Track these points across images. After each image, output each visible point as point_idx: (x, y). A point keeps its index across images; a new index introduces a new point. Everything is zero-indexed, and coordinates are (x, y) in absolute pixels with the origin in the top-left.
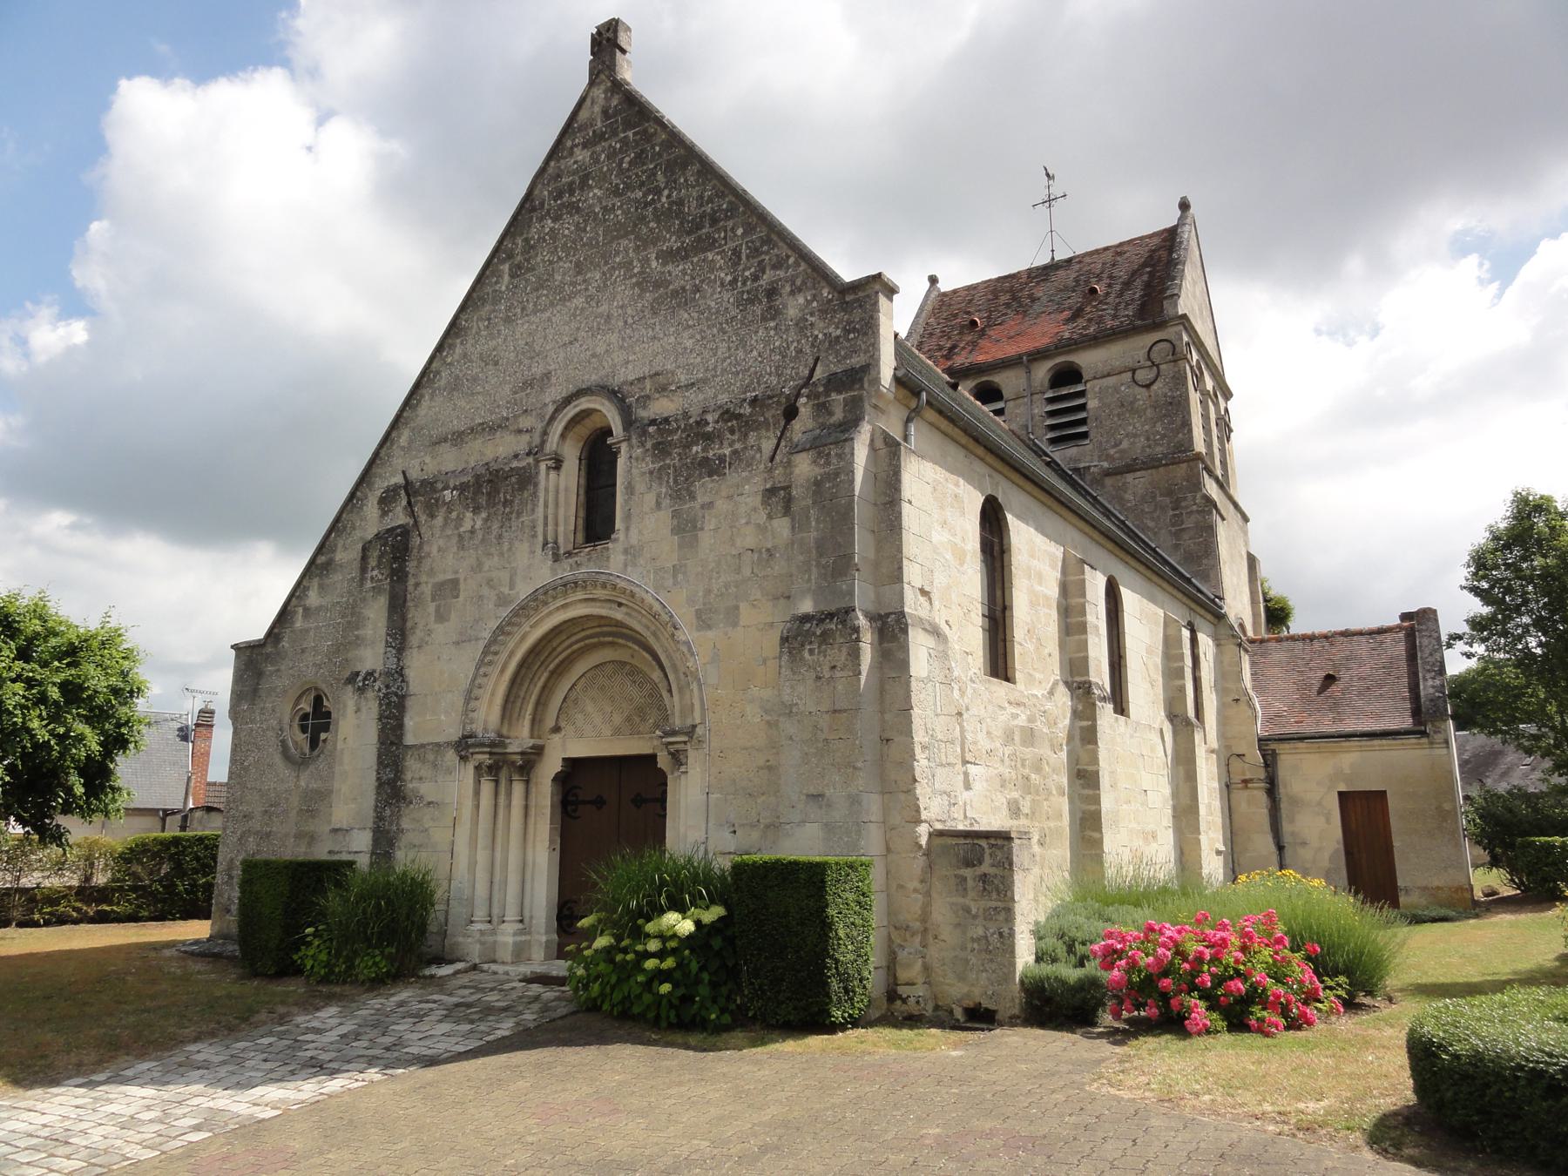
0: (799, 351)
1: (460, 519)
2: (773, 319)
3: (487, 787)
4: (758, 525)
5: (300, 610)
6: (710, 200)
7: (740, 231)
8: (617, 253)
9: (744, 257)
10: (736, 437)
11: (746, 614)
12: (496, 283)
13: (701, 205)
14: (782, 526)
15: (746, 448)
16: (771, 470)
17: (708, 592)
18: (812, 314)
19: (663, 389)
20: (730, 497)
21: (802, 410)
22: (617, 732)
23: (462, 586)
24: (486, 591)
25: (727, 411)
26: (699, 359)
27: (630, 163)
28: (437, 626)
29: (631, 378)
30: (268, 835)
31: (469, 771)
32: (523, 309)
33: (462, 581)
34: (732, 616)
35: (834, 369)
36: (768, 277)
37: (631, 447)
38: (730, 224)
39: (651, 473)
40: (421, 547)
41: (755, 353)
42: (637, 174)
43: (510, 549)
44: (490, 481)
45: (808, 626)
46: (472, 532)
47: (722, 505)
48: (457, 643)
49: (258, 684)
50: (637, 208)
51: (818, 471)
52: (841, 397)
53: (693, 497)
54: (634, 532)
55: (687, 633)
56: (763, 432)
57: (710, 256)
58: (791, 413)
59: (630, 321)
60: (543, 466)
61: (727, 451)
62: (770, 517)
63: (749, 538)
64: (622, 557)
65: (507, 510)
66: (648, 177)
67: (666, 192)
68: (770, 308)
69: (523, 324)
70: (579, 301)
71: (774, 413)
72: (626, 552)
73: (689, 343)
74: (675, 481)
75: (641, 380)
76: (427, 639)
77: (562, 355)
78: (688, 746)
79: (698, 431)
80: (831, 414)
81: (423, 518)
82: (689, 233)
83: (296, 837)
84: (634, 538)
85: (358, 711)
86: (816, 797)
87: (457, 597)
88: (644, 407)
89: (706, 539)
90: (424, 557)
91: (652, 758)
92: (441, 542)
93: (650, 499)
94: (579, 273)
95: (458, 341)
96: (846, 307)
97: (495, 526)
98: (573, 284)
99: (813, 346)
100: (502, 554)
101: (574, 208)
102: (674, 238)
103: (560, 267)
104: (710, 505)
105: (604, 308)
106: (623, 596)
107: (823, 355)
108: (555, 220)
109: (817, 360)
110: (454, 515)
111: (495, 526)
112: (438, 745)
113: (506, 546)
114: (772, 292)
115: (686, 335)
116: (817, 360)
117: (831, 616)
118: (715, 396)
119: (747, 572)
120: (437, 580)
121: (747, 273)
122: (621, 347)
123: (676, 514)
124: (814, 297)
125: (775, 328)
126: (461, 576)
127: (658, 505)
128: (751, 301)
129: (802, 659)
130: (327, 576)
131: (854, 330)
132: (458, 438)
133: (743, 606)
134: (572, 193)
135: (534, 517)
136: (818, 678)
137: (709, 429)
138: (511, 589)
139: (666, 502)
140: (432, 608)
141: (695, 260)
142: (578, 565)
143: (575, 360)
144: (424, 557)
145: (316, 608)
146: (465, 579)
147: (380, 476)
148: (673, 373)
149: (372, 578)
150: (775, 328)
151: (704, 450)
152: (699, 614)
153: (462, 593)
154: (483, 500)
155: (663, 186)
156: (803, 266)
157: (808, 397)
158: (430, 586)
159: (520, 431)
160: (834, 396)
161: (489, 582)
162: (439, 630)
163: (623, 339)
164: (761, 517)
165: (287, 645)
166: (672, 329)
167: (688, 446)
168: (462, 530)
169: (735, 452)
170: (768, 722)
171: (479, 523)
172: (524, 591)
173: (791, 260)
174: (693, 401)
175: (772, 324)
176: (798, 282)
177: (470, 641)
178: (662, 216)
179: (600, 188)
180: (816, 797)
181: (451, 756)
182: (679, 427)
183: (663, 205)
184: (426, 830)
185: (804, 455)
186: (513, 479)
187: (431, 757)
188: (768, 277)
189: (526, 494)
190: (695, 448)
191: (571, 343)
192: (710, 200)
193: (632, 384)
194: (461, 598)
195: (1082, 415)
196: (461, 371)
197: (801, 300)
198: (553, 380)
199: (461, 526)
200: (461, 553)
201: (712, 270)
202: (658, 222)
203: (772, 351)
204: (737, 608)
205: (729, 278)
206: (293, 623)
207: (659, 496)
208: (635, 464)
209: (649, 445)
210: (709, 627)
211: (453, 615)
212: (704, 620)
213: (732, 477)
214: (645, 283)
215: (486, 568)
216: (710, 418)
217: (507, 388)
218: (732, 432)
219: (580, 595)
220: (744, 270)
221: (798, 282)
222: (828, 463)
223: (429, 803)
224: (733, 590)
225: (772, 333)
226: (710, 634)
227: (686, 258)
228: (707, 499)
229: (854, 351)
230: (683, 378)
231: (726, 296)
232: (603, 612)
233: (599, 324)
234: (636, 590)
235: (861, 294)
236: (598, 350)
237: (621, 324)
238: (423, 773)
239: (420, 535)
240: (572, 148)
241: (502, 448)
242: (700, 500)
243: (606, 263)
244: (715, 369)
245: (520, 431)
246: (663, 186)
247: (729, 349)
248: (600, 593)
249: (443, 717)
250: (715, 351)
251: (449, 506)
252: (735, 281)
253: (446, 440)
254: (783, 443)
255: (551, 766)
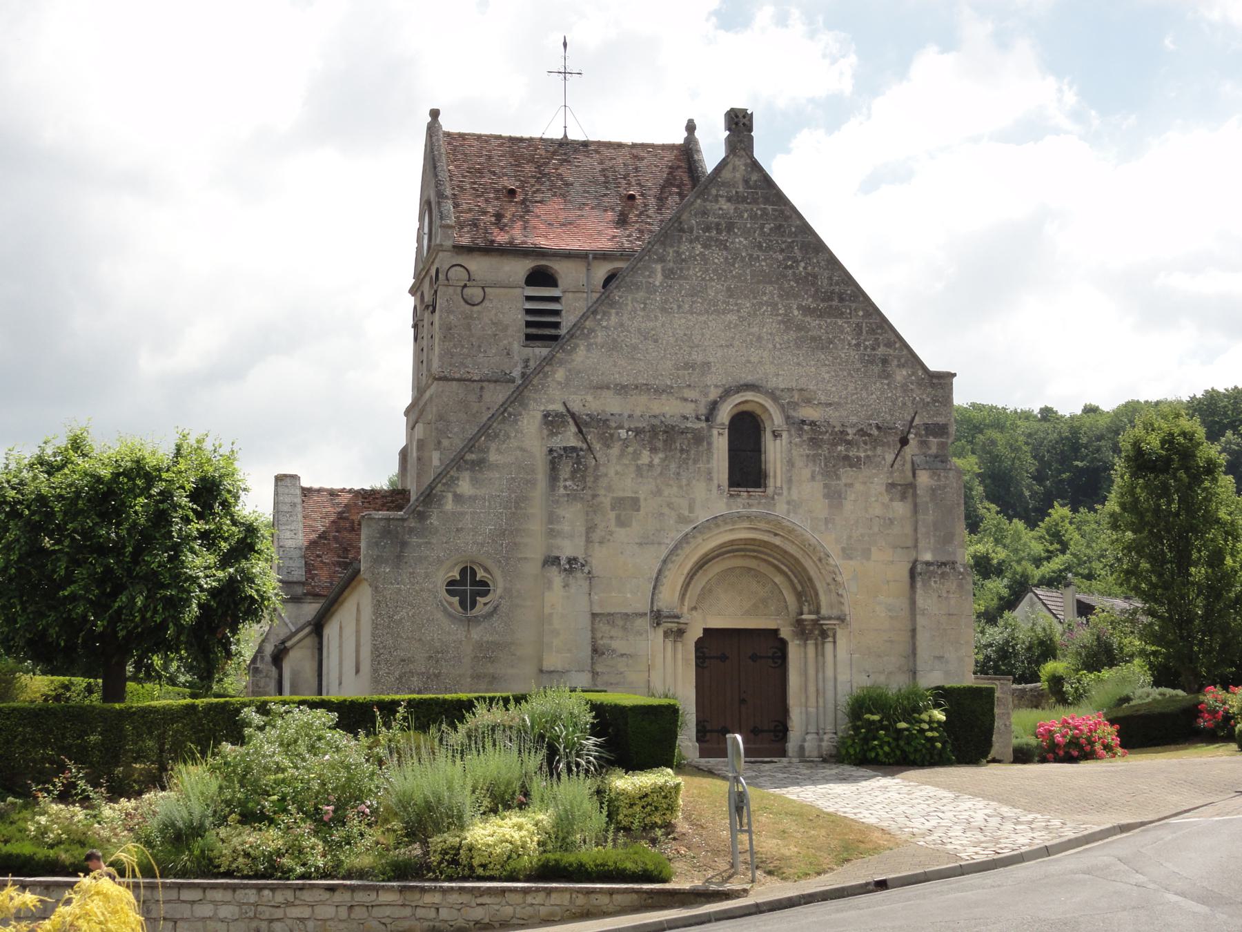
0: (904, 404)
1: (636, 455)
2: (886, 378)
3: (669, 645)
4: (883, 504)
5: (450, 496)
6: (837, 284)
7: (861, 313)
8: (765, 294)
9: (864, 332)
10: (868, 447)
11: (875, 554)
12: (649, 277)
13: (831, 285)
14: (901, 509)
15: (875, 456)
16: (891, 473)
17: (850, 537)
18: (912, 384)
19: (808, 401)
20: (865, 483)
21: (911, 441)
22: (748, 613)
23: (642, 503)
24: (666, 510)
25: (862, 430)
26: (834, 389)
27: (771, 229)
28: (618, 529)
29: (782, 386)
30: (437, 676)
31: (660, 632)
32: (679, 307)
33: (642, 500)
34: (867, 554)
35: (926, 421)
36: (881, 350)
37: (791, 436)
38: (854, 305)
39: (808, 456)
40: (597, 467)
41: (874, 396)
42: (777, 242)
43: (688, 485)
44: (665, 432)
45: (932, 568)
46: (651, 465)
47: (858, 487)
48: (641, 544)
49: (401, 551)
50: (779, 267)
51: (932, 482)
52: (935, 440)
53: (838, 478)
54: (794, 492)
55: (836, 560)
56: (886, 449)
57: (840, 322)
58: (904, 442)
59: (778, 346)
60: (715, 432)
61: (862, 455)
62: (891, 500)
63: (877, 510)
64: (785, 506)
65: (684, 456)
66: (788, 247)
67: (802, 264)
68: (884, 371)
69: (680, 319)
70: (733, 318)
71: (894, 439)
72: (788, 503)
73: (827, 376)
74: (826, 465)
75: (790, 390)
76: (609, 537)
77: (719, 354)
78: (837, 627)
79: (840, 437)
80: (929, 448)
81: (597, 446)
82: (823, 300)
83: (472, 677)
84: (795, 496)
85: (566, 586)
86: (940, 658)
87: (638, 510)
88: (794, 410)
89: (848, 506)
90: (601, 476)
91: (776, 631)
92: (618, 468)
93: (807, 473)
94: (730, 296)
95: (613, 311)
96: (933, 385)
97: (673, 466)
98: (728, 304)
99: (913, 403)
100: (680, 487)
101: (723, 245)
102: (810, 300)
103: (713, 286)
104: (851, 485)
105: (755, 329)
106: (777, 526)
107: (919, 411)
108: (705, 246)
109: (916, 413)
110: (630, 449)
111: (673, 466)
112: (626, 614)
113: (684, 482)
114: (885, 361)
115: (824, 369)
116: (916, 413)
117: (944, 564)
118: (848, 417)
119: (876, 529)
120: (615, 495)
121: (867, 343)
122: (772, 363)
123: (826, 486)
124: (913, 374)
125: (888, 385)
126: (642, 497)
127: (813, 478)
128: (872, 362)
129: (930, 585)
130: (481, 470)
131: (938, 401)
132: (622, 389)
133: (873, 549)
134: (719, 232)
135: (710, 466)
136: (939, 596)
137: (850, 437)
138: (690, 512)
139: (819, 477)
140: (612, 515)
141: (829, 321)
142: (750, 506)
143: (732, 360)
144: (601, 476)
145: (470, 497)
146: (646, 499)
147: (535, 400)
148: (815, 392)
149: (565, 487)
150: (888, 385)
151: (846, 450)
152: (843, 549)
153: (642, 509)
154: (660, 445)
155: (800, 258)
156: (905, 352)
157: (915, 435)
158: (609, 499)
159: (686, 400)
160: (931, 439)
161: (670, 505)
162: (621, 533)
163: (774, 358)
164: (886, 499)
165: (436, 523)
166: (813, 363)
167: (836, 445)
168: (639, 462)
169: (868, 457)
170: (890, 617)
171: (656, 461)
172: (703, 516)
173: (897, 345)
174: (834, 416)
175: (886, 382)
176: (903, 360)
177: (653, 544)
178: (802, 280)
179: (746, 239)
180: (940, 658)
181: (641, 624)
182: (827, 432)
183: (800, 272)
184: (621, 673)
185: (924, 471)
186: (689, 436)
187: (621, 623)
188: (881, 350)
189: (701, 448)
190: (839, 448)
191: (727, 346)
192: (837, 284)
193: (782, 390)
194: (642, 512)
195: (553, 332)
196: (619, 336)
197: (904, 373)
198: (713, 369)
199: (639, 459)
200: (640, 480)
201: (842, 332)
202: (797, 282)
203: (886, 398)
204: (870, 550)
205: (854, 342)
206: (440, 505)
207: (813, 472)
208: (794, 447)
209: (805, 437)
210: (851, 559)
211: (634, 523)
212: (847, 553)
213: (866, 472)
214: (787, 323)
215: (666, 493)
216: (849, 431)
217: (669, 364)
218: (865, 443)
219: (746, 525)
220: (865, 340)
221: (903, 360)
222: (939, 479)
223: (622, 655)
224: (866, 538)
225: (886, 387)
226: (851, 562)
227: (820, 316)
228: (849, 481)
229: (938, 414)
230: (823, 398)
231: (853, 353)
232: (766, 537)
233: (751, 340)
234: (796, 527)
235: (942, 381)
236: (752, 359)
237: (771, 346)
238: (613, 633)
239: (595, 458)
240: (717, 196)
241: (670, 409)
242: (844, 481)
243: (755, 298)
244: (846, 398)
245: (686, 400)
246: (800, 258)
247: (856, 389)
248: (762, 525)
249: (629, 595)
250: (846, 387)
251: (626, 443)
252: (858, 345)
253: (608, 388)
254: (899, 458)
255: (695, 633)
